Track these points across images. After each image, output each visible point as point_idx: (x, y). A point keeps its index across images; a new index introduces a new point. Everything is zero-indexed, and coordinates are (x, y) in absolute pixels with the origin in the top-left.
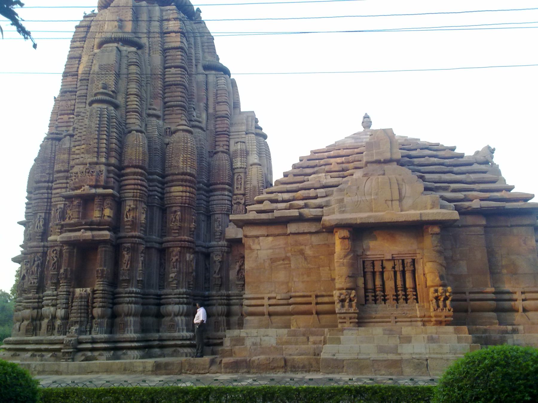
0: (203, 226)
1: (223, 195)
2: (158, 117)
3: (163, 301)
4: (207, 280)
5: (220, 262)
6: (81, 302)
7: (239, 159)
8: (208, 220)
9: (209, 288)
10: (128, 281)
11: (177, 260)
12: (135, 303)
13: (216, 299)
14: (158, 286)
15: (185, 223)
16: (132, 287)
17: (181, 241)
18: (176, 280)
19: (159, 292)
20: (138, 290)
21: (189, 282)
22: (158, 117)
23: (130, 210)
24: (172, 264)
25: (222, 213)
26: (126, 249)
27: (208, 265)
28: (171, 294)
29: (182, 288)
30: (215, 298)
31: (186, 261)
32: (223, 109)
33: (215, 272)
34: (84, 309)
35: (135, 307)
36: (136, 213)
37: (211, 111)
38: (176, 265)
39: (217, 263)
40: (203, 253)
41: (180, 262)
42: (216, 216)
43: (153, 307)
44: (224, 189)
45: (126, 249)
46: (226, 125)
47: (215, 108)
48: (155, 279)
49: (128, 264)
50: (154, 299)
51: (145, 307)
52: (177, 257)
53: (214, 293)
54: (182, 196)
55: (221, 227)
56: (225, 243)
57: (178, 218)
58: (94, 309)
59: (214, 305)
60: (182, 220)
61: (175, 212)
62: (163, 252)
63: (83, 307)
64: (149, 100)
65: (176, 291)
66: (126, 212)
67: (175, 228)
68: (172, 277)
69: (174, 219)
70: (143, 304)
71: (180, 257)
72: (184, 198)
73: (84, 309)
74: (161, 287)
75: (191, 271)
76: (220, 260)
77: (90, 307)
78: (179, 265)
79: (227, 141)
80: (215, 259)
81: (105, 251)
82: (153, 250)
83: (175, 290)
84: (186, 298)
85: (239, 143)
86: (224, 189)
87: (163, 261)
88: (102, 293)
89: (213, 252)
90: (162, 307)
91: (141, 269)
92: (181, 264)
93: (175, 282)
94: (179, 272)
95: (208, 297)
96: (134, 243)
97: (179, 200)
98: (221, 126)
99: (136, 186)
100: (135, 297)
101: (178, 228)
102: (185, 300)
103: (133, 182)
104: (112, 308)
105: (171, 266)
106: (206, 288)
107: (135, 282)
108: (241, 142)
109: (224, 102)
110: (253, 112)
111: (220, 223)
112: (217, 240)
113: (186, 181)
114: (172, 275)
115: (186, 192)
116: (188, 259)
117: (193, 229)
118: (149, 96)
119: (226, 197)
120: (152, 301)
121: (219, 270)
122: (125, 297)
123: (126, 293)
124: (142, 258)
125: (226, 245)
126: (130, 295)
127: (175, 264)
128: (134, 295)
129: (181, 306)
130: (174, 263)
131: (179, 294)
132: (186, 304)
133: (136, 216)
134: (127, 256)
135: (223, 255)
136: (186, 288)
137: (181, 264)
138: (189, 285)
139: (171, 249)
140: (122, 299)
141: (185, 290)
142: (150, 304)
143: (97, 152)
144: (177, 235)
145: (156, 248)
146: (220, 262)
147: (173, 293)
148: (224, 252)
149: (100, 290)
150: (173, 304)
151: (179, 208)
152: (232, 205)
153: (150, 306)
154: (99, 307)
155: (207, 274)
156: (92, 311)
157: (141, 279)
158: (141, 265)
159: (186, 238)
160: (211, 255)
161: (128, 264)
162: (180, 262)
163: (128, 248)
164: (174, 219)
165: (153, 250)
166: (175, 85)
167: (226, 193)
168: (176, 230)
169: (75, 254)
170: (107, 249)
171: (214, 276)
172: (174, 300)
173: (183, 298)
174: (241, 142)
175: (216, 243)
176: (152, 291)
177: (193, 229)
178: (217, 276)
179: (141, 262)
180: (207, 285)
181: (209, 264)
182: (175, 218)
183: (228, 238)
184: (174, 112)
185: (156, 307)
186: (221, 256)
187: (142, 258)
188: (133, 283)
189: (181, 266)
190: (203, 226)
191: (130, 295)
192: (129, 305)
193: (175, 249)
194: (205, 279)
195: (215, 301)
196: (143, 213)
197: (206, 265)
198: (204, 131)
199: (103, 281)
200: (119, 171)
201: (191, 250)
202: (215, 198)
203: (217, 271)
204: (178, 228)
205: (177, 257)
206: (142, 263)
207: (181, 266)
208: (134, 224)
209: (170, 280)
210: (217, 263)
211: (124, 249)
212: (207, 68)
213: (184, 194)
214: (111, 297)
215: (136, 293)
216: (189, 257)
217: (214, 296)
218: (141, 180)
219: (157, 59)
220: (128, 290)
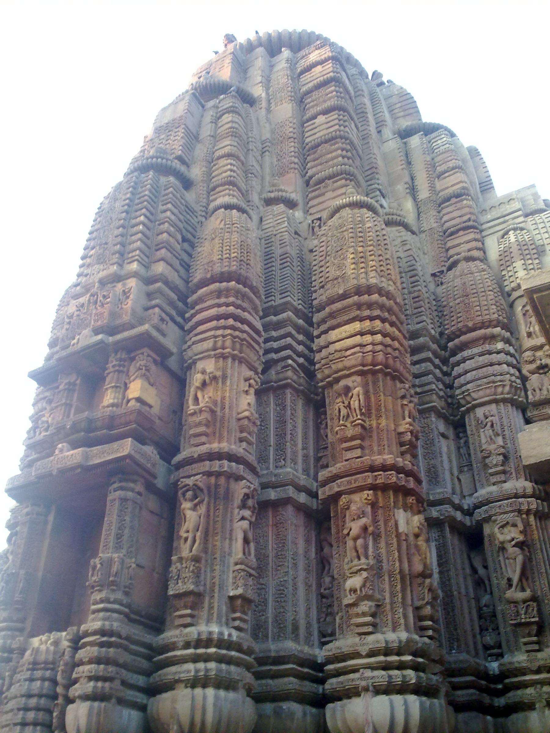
0: (444, 449)
1: (490, 353)
2: (291, 204)
3: (332, 683)
4: (488, 619)
5: (521, 545)
6: (31, 680)
7: (519, 264)
8: (458, 437)
9: (500, 647)
10: (195, 599)
11: (365, 529)
12: (224, 684)
13: (533, 684)
14: (316, 634)
15: (379, 417)
16: (209, 621)
17: (372, 469)
18: (369, 598)
19: (321, 654)
20: (230, 633)
21: (417, 609)
22: (291, 204)
23: (204, 384)
24: (350, 543)
25: (496, 401)
26: (189, 494)
27: (481, 571)
28: (356, 655)
29: (394, 630)
30: (527, 678)
31: (398, 535)
32: (451, 183)
33: (509, 580)
34: (37, 709)
35: (216, 697)
36: (223, 391)
37: (424, 194)
38: (366, 547)
39: (511, 550)
40: (456, 528)
41: (376, 536)
42: (480, 412)
43: (296, 708)
44: (493, 338)
45: (189, 494)
46: (467, 210)
47: (432, 188)
48: (302, 606)
49: (194, 541)
50: (301, 677)
51: (268, 707)
52: (364, 521)
53: (520, 658)
54: (361, 346)
55: (500, 441)
56: (523, 484)
57: (355, 404)
58: (70, 707)
59: (531, 707)
60: (367, 412)
61: (347, 390)
62: (322, 519)
63: (33, 702)
64: (267, 178)
65: (376, 640)
66: (192, 390)
67: (350, 433)
68: (353, 591)
69: (344, 412)
70: (259, 698)
71: (375, 521)
72: (370, 348)
73: (37, 709)
74: (326, 636)
75: (418, 568)
76: (521, 538)
77: (60, 701)
78: (376, 548)
79: (476, 240)
80: (501, 538)
81: (124, 500)
82: (290, 509)
83: (371, 638)
84: (416, 668)
85: (511, 232)
86: (493, 338)
87: (326, 550)
88: (102, 645)
89: (488, 520)
90: (330, 706)
91: (240, 555)
92: (383, 544)
93: (366, 606)
94: (377, 571)
95: (503, 675)
96: (218, 474)
97: (353, 360)
98: (453, 215)
99: (222, 322)
100: (220, 660)
101: (359, 430)
102: (410, 673)
103: (213, 312)
104: (143, 708)
105: (350, 553)
106: (486, 648)
107: (219, 604)
108: (515, 229)
109: (453, 169)
110: (533, 186)
111: (498, 428)
112: (493, 479)
113: (370, 306)
114: (355, 582)
115: (373, 333)
116: (402, 528)
117: (408, 437)
118: (267, 170)
119: (502, 357)
120: (290, 683)
121: (523, 574)
122: (183, 660)
123: (187, 645)
124: (245, 524)
125: (529, 491)
126: (201, 651)
127: (360, 542)
128: (212, 650)
129: (398, 699)
130: (355, 539)
131: (387, 652)
132: (417, 690)
133: (223, 398)
134: (191, 516)
135: (527, 524)
136: (407, 629)
137: (383, 544)
138: (421, 619)
139: (343, 500)
140: (173, 669)
141: (404, 635)
142: (285, 697)
143: (122, 254)
144: (358, 452)
145: (300, 508)
146: (521, 545)
147: (364, 651)
148: (528, 512)
149: (94, 633)
150: (366, 689)
151: (358, 379)
152: (524, 379)
153: (285, 705)
154: (86, 698)
155: (485, 599)
156: (63, 714)
157: (240, 591)
158: (239, 544)
159: (389, 458)
160: (487, 530)
161: (194, 541)
162: (376, 536)
163: (196, 489)
164: (344, 412)
165: (290, 509)
166: (326, 142)
167: (500, 345)
168: (353, 438)
169: (49, 527)
170: (130, 494)
171: (510, 594)
172: (368, 673)
173: (401, 666)
174: (515, 229)
175: (493, 488)
176: (290, 646)
177: (408, 437)
178: (521, 596)
179: (240, 536)
180: (489, 639)
181: (486, 567)
182: (347, 405)
183: (532, 461)
184: (329, 188)
185: (314, 710)
186: (521, 527)
187: (245, 524)
188: (211, 608)
189: (383, 551)
190: (444, 449)
191: (201, 651)
192: (198, 691)
193: (356, 497)
194: (480, 617)
195: (530, 691)
196: (247, 392)
197: (474, 571)
198: (413, 233)
199: (106, 600)
200: (181, 303)
201: (411, 500)
202: (468, 365)
203: (515, 579)
204: (359, 430)
205: (364, 521)
206: (246, 541)
207: (383, 551)
208: (215, 420)
209: (348, 600)
210: (511, 550)
211: (184, 494)
212: (405, 134)
213: (368, 338)
214: (145, 664)
215: (221, 643)
216: (407, 521)
217: (523, 672)
218: (237, 307)
219: (285, 111)
220: (192, 632)
